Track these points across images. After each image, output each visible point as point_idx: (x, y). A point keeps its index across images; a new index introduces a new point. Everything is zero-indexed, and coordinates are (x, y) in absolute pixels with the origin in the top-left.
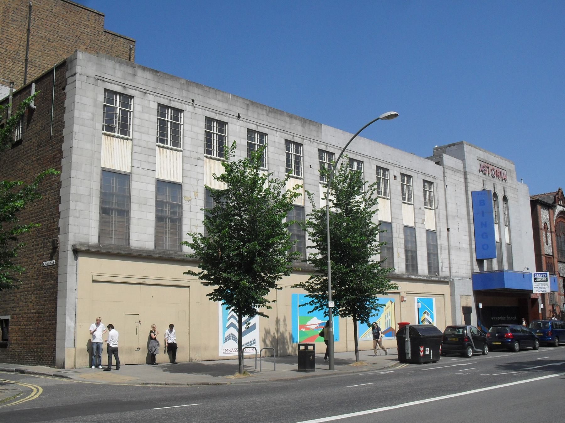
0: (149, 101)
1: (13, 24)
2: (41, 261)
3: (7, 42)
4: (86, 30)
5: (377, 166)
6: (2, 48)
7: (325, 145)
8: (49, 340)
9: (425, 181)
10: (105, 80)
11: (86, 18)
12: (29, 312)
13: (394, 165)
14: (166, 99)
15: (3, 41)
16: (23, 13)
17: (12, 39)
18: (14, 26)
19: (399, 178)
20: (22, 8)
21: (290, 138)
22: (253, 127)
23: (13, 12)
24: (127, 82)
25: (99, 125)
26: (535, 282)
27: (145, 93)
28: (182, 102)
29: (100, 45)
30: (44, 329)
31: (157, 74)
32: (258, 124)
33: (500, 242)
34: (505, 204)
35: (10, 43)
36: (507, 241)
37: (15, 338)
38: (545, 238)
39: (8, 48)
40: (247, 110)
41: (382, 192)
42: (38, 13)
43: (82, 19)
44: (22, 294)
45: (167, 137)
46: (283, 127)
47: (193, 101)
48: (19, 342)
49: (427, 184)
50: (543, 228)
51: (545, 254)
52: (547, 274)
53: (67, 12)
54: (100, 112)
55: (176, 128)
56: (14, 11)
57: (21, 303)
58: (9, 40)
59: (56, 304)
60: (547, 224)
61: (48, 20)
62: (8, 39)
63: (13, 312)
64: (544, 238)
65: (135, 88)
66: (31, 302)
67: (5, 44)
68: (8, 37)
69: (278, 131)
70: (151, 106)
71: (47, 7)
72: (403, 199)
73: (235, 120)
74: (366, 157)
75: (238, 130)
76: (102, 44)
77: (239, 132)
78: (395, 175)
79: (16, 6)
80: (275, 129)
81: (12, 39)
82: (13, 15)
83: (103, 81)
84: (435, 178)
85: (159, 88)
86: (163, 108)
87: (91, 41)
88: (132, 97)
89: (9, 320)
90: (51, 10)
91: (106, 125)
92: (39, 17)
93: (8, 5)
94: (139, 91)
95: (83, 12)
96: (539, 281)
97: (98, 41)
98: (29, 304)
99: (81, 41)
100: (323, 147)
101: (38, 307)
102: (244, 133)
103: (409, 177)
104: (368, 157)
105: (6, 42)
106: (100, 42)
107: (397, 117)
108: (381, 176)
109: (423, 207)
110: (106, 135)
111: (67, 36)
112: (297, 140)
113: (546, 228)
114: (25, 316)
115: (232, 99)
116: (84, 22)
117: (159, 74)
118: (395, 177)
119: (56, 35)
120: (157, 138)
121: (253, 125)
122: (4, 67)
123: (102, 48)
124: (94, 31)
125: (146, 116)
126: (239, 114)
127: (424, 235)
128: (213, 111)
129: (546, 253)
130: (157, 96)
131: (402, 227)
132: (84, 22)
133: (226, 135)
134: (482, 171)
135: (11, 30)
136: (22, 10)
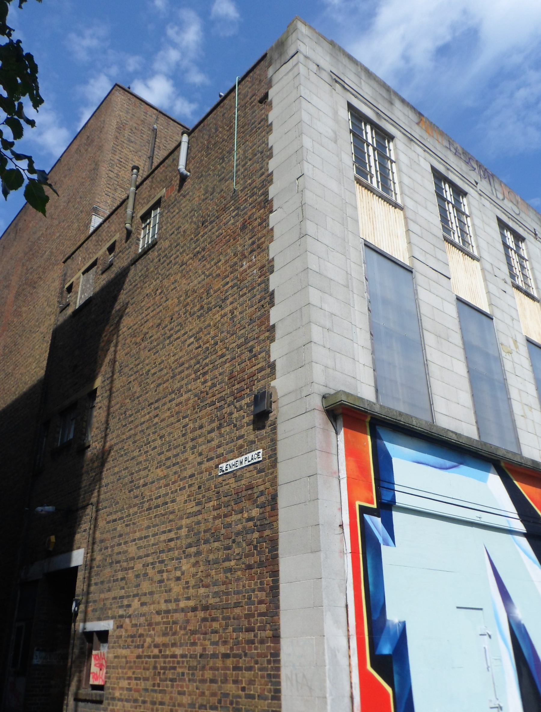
1: (130, 146)
2: (212, 464)
6: (112, 171)
8: (250, 697)
12: (172, 606)
15: (113, 162)
16: (144, 136)
18: (131, 148)
20: (143, 129)
23: (130, 131)
27: (412, 140)
30: (226, 656)
35: (123, 168)
37: (124, 683)
39: (120, 174)
42: (165, 142)
44: (150, 559)
48: (136, 695)
56: (132, 130)
57: (146, 586)
58: (122, 164)
59: (275, 574)
62: (121, 162)
63: (121, 612)
66: (178, 579)
67: (117, 168)
68: (121, 160)
79: (135, 125)
82: (130, 134)
83: (344, 87)
89: (110, 633)
92: (165, 146)
98: (172, 584)
101: (202, 591)
105: (118, 165)
114: (158, 618)
122: (113, 198)
128: (505, 212)
135: (126, 152)
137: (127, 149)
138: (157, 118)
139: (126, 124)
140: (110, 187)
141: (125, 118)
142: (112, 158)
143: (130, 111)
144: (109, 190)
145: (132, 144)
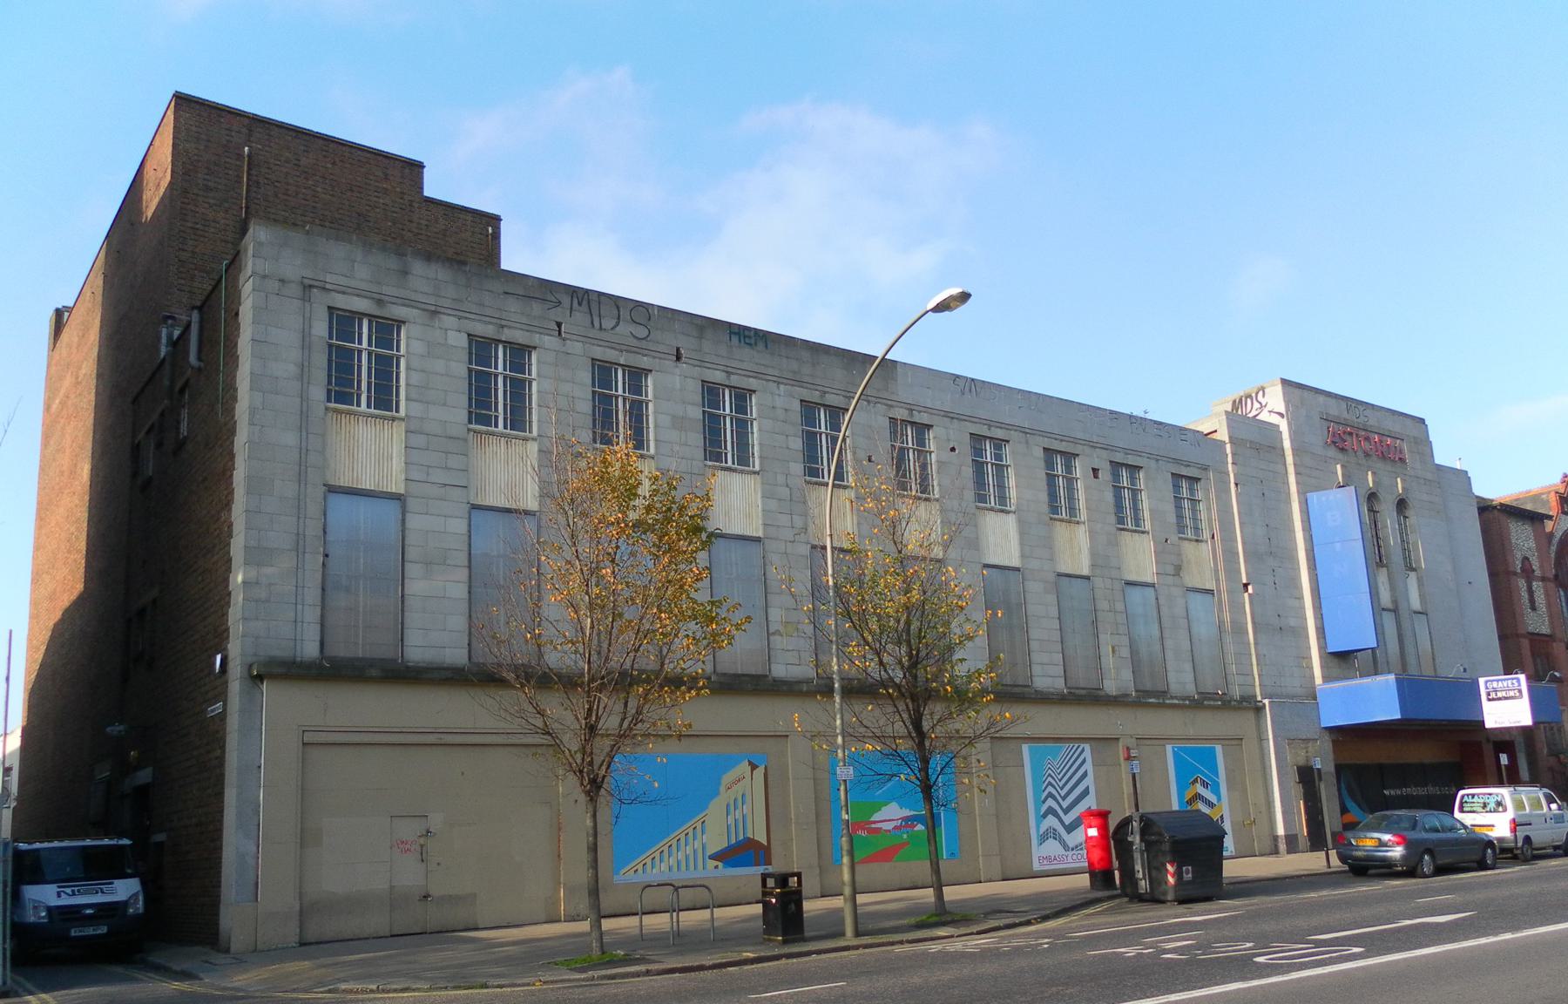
0: (446, 330)
3: (196, 238)
4: (381, 201)
5: (1045, 449)
6: (183, 250)
7: (908, 409)
9: (1176, 477)
10: (328, 286)
11: (380, 174)
13: (1093, 446)
14: (490, 323)
16: (230, 172)
17: (206, 229)
18: (212, 201)
19: (1105, 475)
20: (228, 160)
21: (814, 396)
22: (718, 376)
23: (206, 171)
24: (386, 290)
25: (318, 393)
26: (1489, 700)
28: (530, 329)
29: (416, 231)
31: (463, 268)
32: (729, 369)
33: (1395, 610)
34: (1405, 517)
35: (202, 239)
36: (1416, 603)
38: (1526, 596)
39: (197, 250)
40: (700, 337)
41: (1063, 508)
42: (267, 171)
43: (372, 177)
45: (496, 410)
46: (794, 372)
47: (559, 325)
49: (1184, 484)
50: (1519, 571)
51: (1533, 634)
52: (1518, 680)
53: (334, 163)
54: (320, 360)
55: (518, 390)
61: (288, 184)
62: (197, 229)
64: (1525, 595)
65: (408, 303)
67: (191, 242)
68: (198, 226)
69: (782, 383)
70: (451, 342)
71: (287, 154)
72: (1121, 520)
73: (669, 363)
74: (1016, 430)
75: (678, 386)
76: (421, 229)
77: (681, 390)
80: (775, 379)
81: (206, 229)
82: (206, 177)
84: (1205, 469)
85: (469, 299)
86: (480, 349)
87: (394, 224)
88: (400, 323)
90: (297, 162)
91: (337, 388)
93: (196, 157)
94: (418, 308)
95: (372, 161)
96: (1499, 699)
97: (411, 221)
99: (371, 224)
100: (900, 414)
102: (694, 392)
103: (1134, 469)
104: (1024, 431)
105: (193, 237)
106: (415, 225)
107: (970, 301)
108: (1060, 470)
109: (1173, 538)
110: (336, 411)
111: (337, 216)
112: (832, 400)
113: (1528, 572)
115: (659, 316)
116: (377, 184)
117: (468, 268)
118: (1095, 471)
119: (311, 215)
120: (470, 413)
121: (718, 372)
123: (420, 237)
124: (401, 201)
125: (439, 365)
126: (678, 349)
129: (1530, 629)
130: (466, 318)
131: (1118, 586)
132: (377, 184)
133: (650, 397)
134: (1334, 443)
136: (228, 165)
137: (206, 205)
138: (250, 131)
139: (199, 161)
140: (184, 275)
141: (196, 151)
142: (182, 228)
143: (203, 136)
144: (183, 282)
145: (211, 195)
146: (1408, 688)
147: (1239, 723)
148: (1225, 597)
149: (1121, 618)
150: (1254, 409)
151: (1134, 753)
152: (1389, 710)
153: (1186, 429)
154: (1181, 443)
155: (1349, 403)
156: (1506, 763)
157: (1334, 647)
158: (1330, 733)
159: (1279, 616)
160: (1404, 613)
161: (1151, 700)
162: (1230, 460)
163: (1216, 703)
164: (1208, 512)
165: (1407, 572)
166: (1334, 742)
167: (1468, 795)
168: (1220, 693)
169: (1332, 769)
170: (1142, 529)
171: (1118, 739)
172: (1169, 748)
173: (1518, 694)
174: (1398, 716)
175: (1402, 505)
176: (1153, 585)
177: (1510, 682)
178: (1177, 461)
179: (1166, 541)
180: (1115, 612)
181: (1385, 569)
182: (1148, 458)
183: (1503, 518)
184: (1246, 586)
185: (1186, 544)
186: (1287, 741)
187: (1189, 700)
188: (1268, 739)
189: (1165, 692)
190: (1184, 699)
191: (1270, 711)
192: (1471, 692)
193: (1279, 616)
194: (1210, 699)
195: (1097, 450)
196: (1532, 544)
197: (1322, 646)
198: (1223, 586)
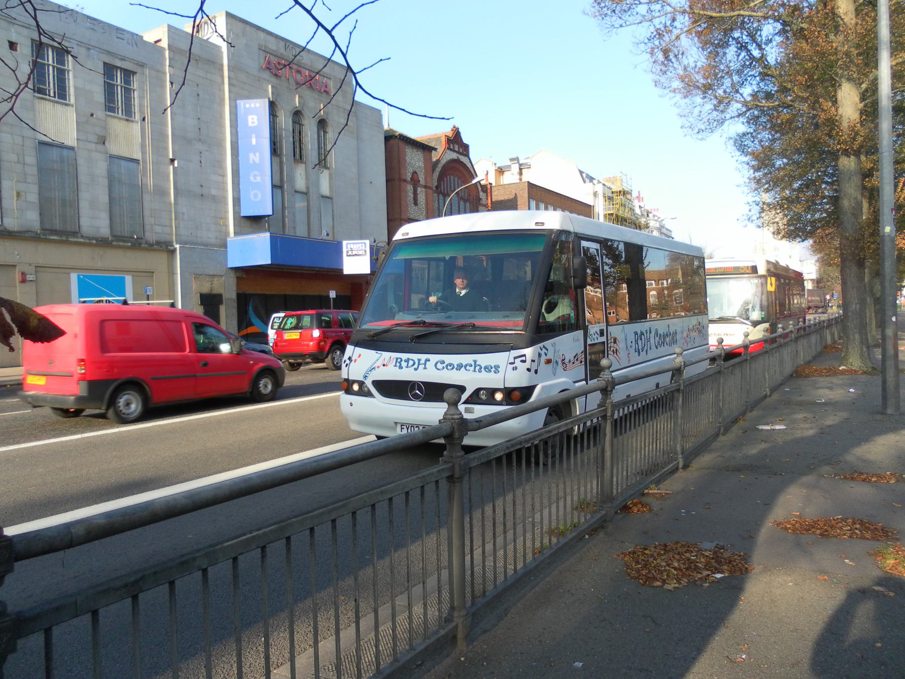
19: (25, 50)
38: (412, 196)
50: (409, 178)
60: (418, 176)
64: (411, 195)
78: (14, 40)
84: (142, 65)
96: (354, 255)
109: (100, 113)
113: (415, 181)
127: (101, 168)
146: (276, 244)
147: (157, 261)
148: (149, 166)
149: (33, 171)
150: (209, 32)
151: (29, 277)
152: (263, 257)
153: (124, 30)
154: (116, 39)
155: (287, 44)
156: (335, 297)
157: (245, 212)
158: (235, 272)
159: (201, 186)
160: (313, 196)
161: (52, 237)
162: (167, 63)
163: (126, 244)
164: (141, 99)
165: (322, 169)
166: (238, 279)
167: (277, 317)
168: (135, 237)
169: (234, 296)
170: (67, 102)
171: (15, 266)
172: (74, 277)
173: (364, 253)
174: (269, 262)
175: (322, 124)
176: (72, 148)
177: (360, 244)
178: (109, 53)
179: (92, 115)
180: (24, 164)
181: (303, 165)
182: (78, 45)
183: (401, 144)
184: (172, 161)
185: (116, 121)
186: (191, 274)
187: (96, 240)
188: (177, 274)
189: (76, 233)
190: (89, 238)
191: (180, 253)
192: (336, 249)
193: (201, 186)
194: (118, 241)
195: (16, 26)
196: (421, 164)
197: (236, 213)
198: (149, 157)
